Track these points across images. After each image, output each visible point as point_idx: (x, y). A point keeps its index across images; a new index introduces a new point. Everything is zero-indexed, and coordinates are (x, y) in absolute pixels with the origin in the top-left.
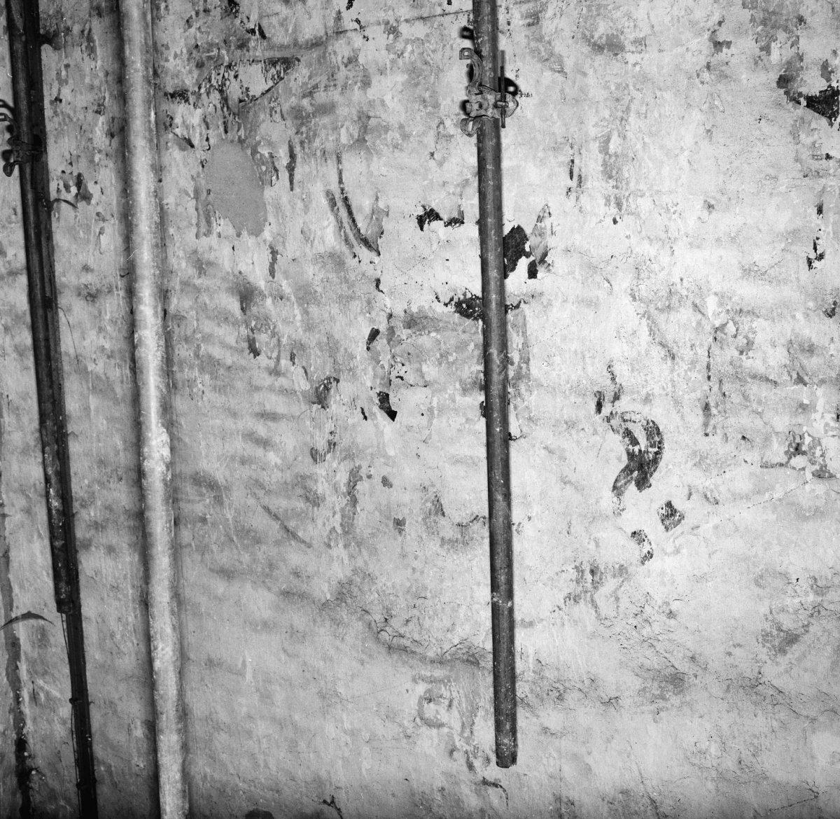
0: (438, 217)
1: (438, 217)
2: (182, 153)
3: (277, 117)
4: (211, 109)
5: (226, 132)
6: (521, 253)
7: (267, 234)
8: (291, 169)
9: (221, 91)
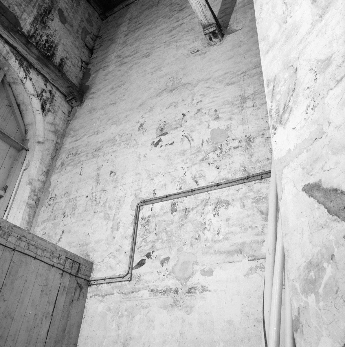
0: (170, 144)
1: (170, 144)
2: (236, 137)
3: (205, 150)
4: (225, 147)
5: (221, 144)
6: (156, 144)
7: (210, 130)
8: (203, 142)
9: (222, 151)
